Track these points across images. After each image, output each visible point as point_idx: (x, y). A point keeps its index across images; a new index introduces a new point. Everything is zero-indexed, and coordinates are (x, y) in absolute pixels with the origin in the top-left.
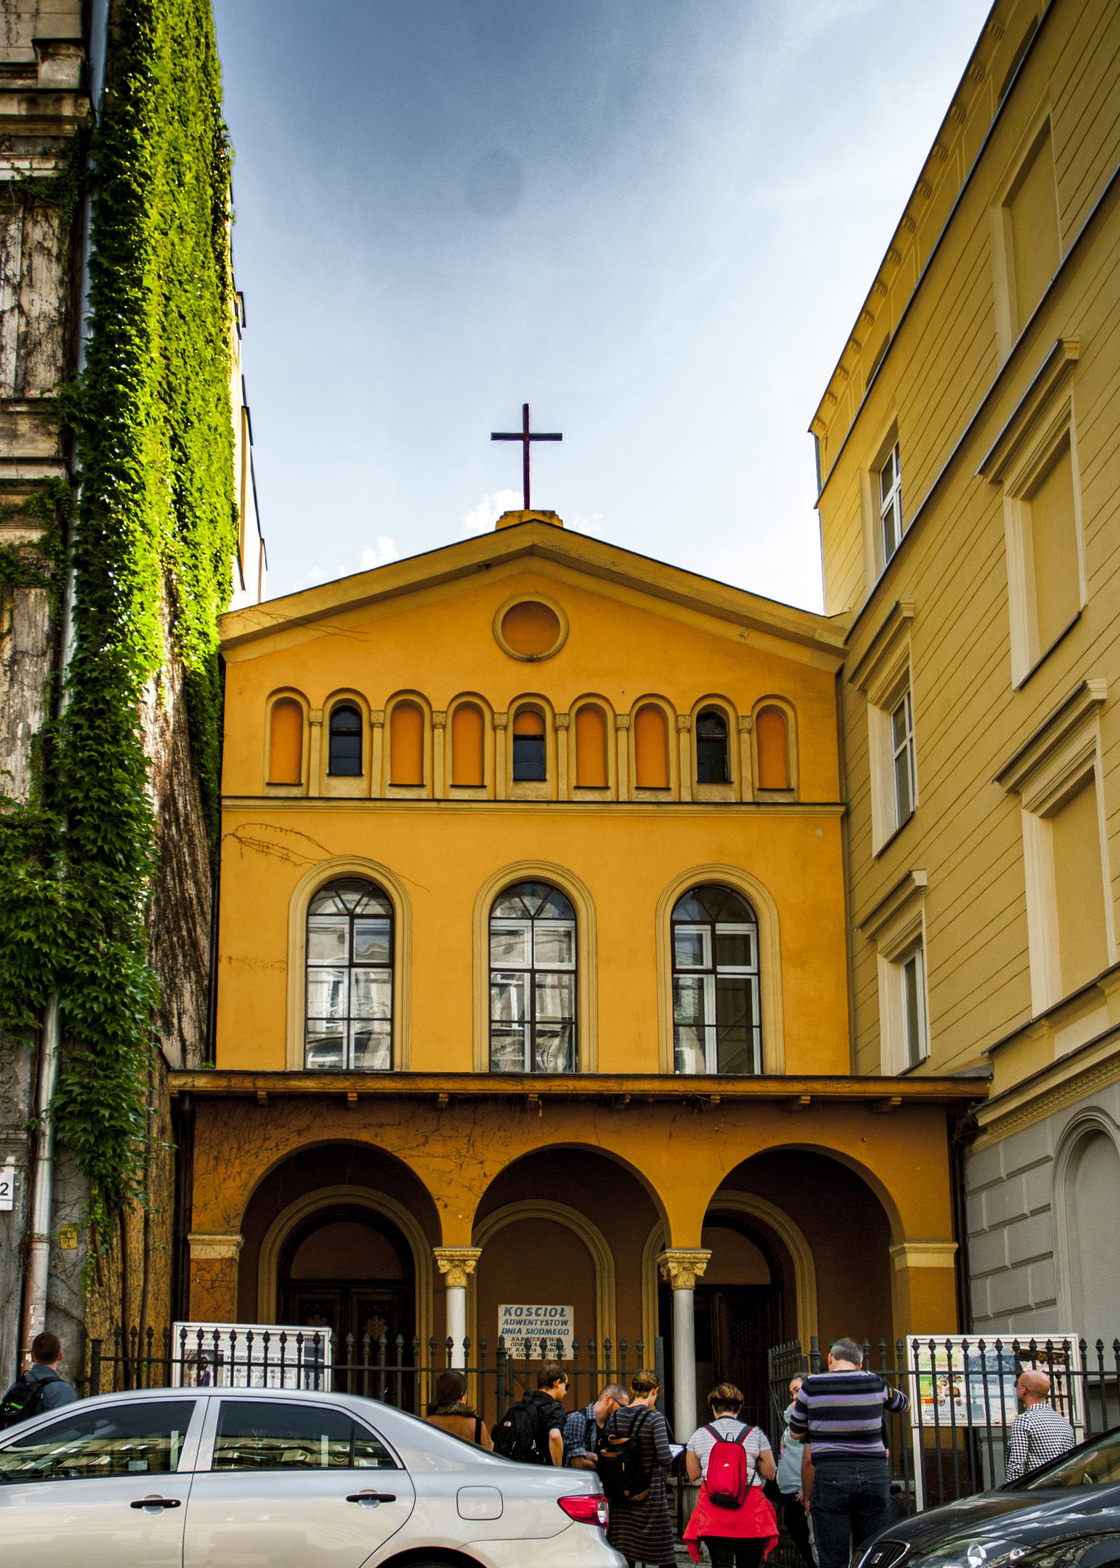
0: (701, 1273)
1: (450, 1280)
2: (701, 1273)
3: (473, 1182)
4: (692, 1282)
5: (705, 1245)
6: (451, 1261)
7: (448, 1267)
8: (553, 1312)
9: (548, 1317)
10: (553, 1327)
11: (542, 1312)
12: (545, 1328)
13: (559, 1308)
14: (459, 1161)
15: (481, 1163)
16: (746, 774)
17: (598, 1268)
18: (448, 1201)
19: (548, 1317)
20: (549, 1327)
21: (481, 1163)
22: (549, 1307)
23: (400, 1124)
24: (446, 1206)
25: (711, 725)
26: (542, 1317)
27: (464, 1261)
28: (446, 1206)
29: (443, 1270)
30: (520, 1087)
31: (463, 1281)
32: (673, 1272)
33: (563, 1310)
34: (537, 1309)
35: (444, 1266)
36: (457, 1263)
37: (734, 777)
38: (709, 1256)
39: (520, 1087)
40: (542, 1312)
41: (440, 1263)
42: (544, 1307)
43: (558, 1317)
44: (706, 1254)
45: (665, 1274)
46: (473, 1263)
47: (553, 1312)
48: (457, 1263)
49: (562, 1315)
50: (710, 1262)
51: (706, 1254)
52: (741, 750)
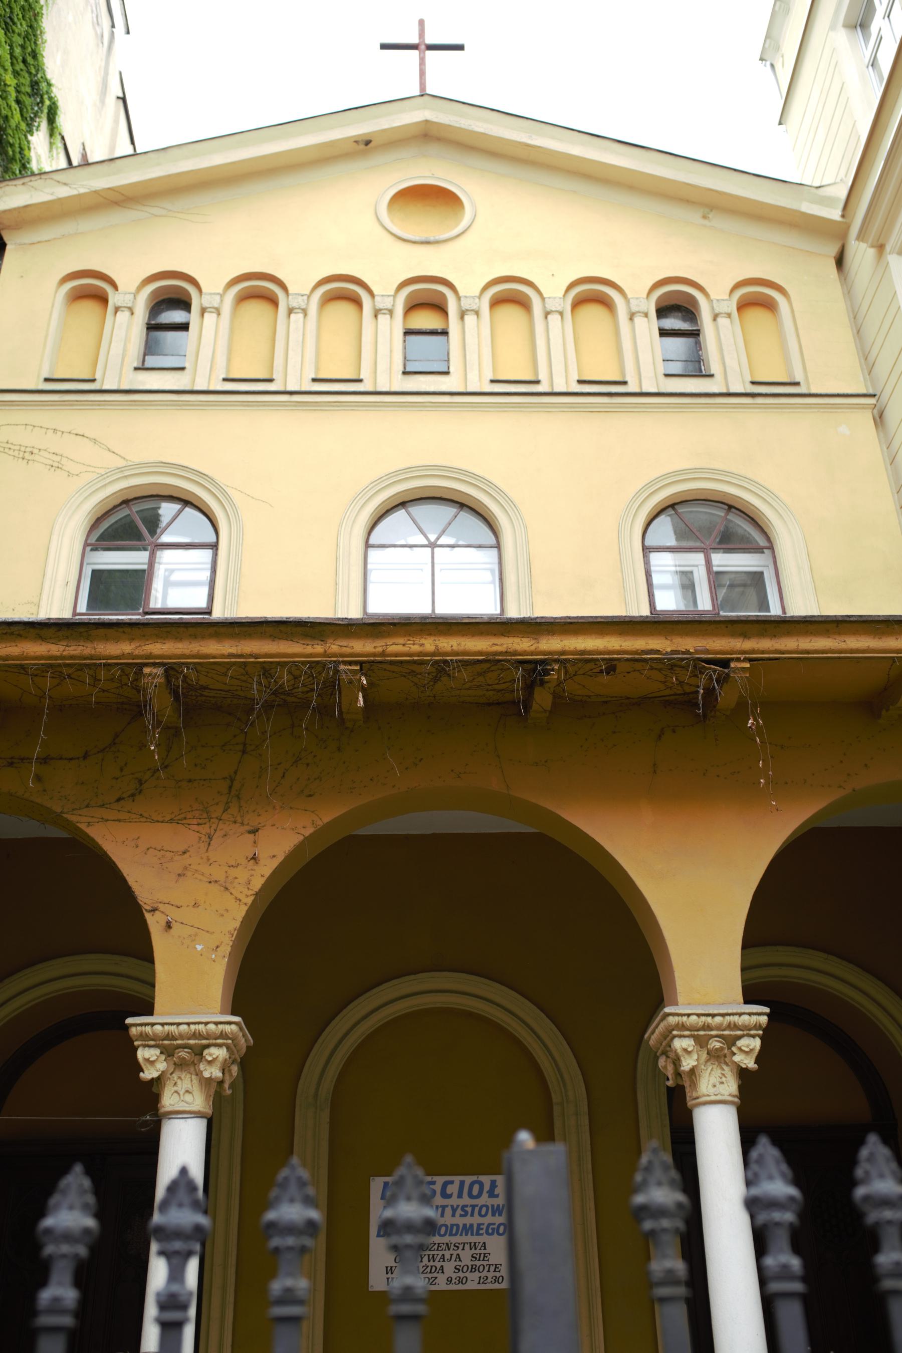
0: (750, 1063)
1: (169, 1100)
2: (750, 1063)
3: (233, 872)
4: (730, 1087)
5: (750, 996)
6: (168, 1052)
7: (162, 1066)
8: (476, 1188)
9: (466, 1200)
10: (476, 1220)
11: (453, 1189)
12: (461, 1221)
13: (486, 1180)
14: (205, 829)
15: (254, 831)
16: (732, 363)
17: (555, 1099)
18: (173, 914)
19: (466, 1200)
20: (468, 1220)
21: (254, 831)
22: (468, 1179)
23: (85, 756)
24: (169, 926)
25: (677, 310)
26: (454, 1201)
27: (198, 1052)
28: (169, 926)
29: (149, 1074)
30: (319, 649)
31: (198, 1101)
32: (687, 1064)
33: (493, 1184)
34: (445, 1185)
35: (151, 1063)
36: (183, 1054)
37: (715, 367)
38: (764, 1020)
39: (319, 649)
40: (453, 1189)
41: (143, 1054)
42: (457, 1179)
43: (484, 1199)
44: (759, 1015)
45: (670, 1071)
46: (220, 1053)
47: (476, 1188)
48: (183, 1054)
49: (492, 1194)
50: (768, 1036)
51: (759, 1015)
52: (722, 337)
